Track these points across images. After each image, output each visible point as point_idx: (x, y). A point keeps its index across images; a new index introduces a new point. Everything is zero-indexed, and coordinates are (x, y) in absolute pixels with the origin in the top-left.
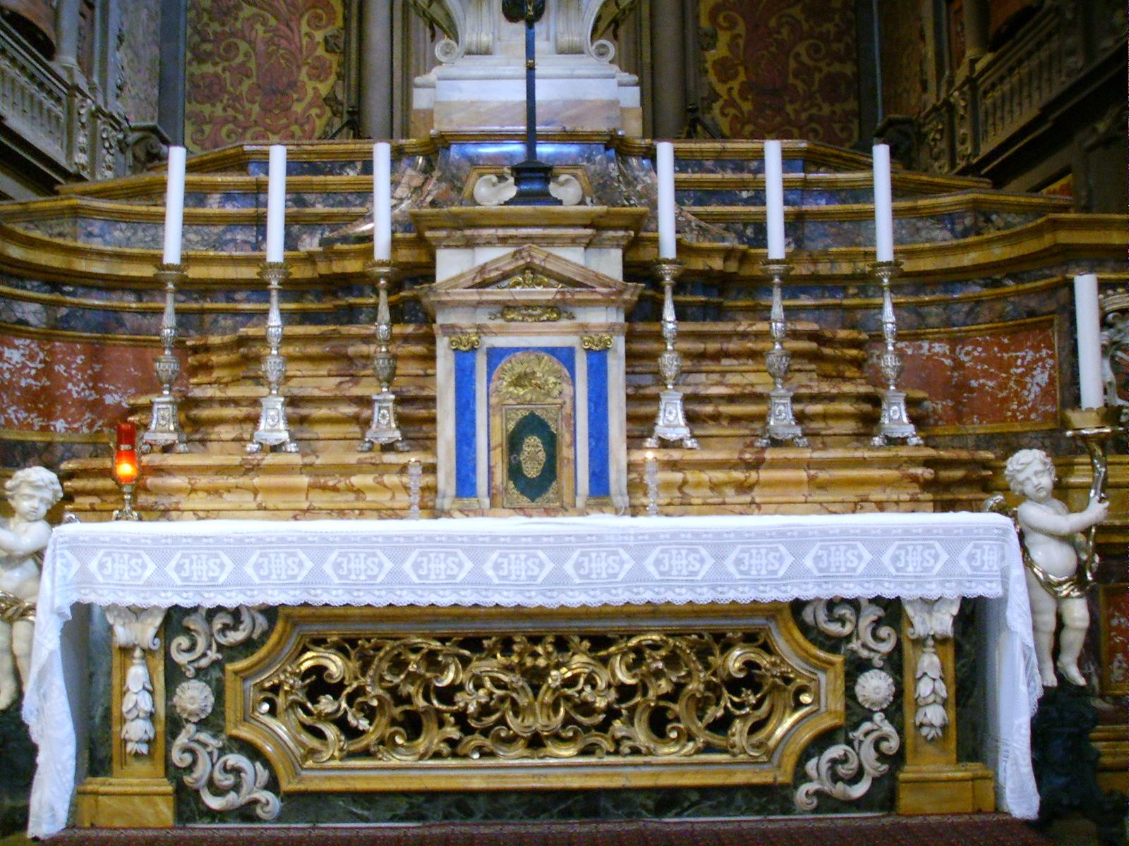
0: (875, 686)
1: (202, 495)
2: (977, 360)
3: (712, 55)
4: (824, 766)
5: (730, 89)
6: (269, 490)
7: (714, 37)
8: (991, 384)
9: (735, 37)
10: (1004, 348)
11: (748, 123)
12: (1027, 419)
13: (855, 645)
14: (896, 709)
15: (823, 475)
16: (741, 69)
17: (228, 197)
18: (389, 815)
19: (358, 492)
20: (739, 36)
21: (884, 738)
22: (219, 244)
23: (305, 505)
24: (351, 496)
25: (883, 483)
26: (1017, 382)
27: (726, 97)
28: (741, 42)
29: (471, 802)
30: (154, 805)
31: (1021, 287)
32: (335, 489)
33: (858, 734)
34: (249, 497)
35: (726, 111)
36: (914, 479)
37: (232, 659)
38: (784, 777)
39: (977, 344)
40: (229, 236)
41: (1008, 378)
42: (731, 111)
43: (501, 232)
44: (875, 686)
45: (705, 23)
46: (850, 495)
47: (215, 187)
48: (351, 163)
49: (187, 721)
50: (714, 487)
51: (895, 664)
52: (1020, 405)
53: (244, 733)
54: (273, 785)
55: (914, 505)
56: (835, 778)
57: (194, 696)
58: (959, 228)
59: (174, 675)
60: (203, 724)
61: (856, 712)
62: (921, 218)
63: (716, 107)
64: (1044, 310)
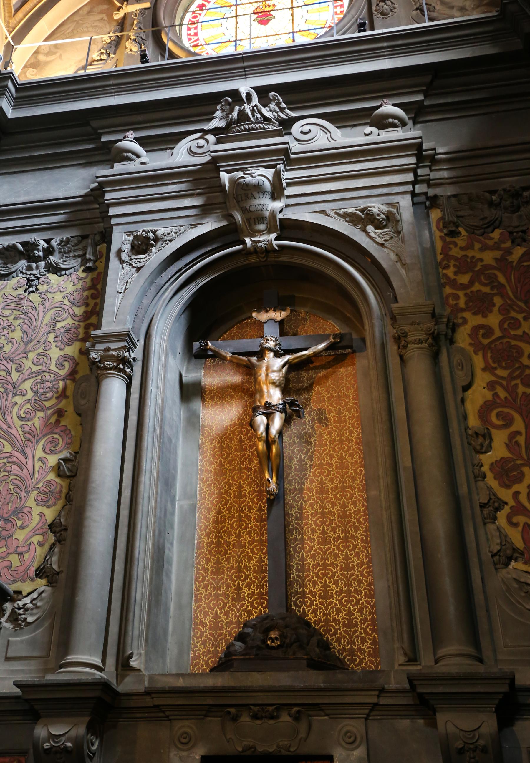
5: (516, 494)
7: (488, 436)
20: (518, 433)
27: (512, 503)
28: (521, 440)
35: (515, 520)
42: (521, 519)
45: (473, 422)
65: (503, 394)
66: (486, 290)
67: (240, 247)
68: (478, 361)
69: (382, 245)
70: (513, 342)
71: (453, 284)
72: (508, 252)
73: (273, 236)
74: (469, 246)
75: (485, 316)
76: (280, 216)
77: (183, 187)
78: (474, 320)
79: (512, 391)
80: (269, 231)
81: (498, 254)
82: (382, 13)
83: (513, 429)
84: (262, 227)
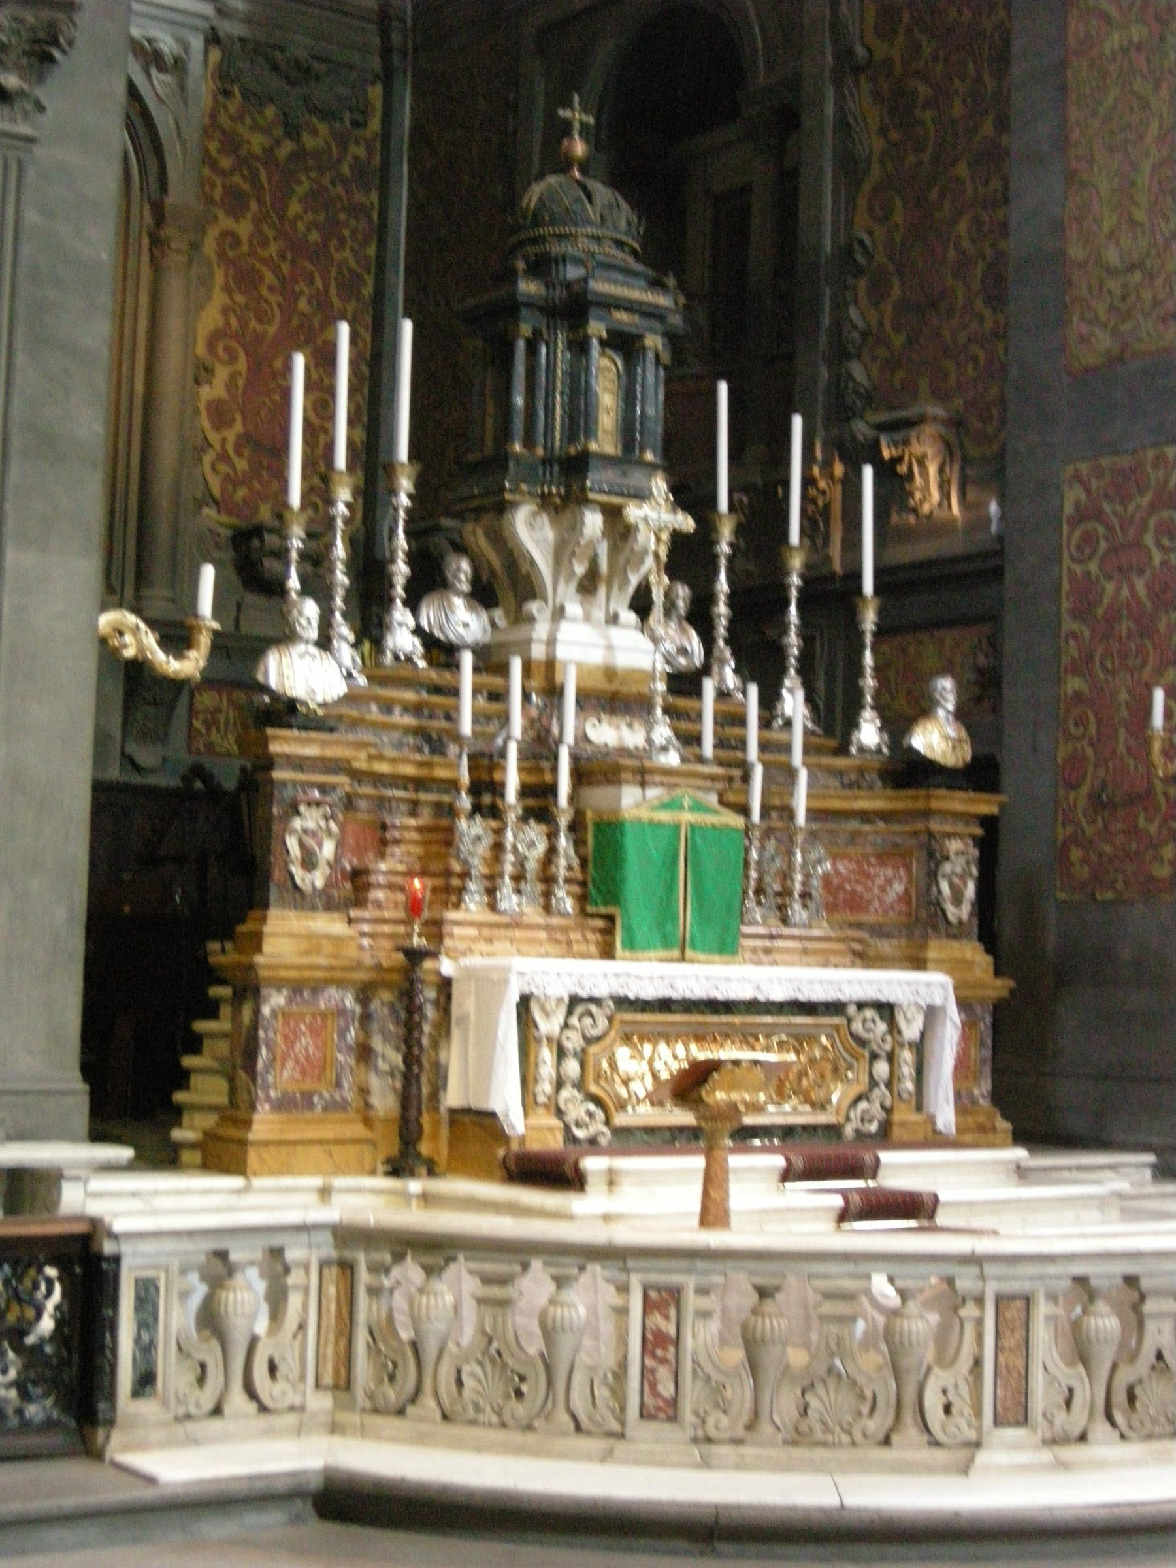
0: (882, 1069)
1: (483, 942)
3: (206, 393)
6: (520, 941)
7: (209, 371)
9: (233, 376)
11: (243, 483)
14: (889, 1085)
15: (810, 945)
16: (238, 417)
27: (218, 447)
28: (241, 382)
34: (507, 945)
38: (841, 1120)
42: (223, 468)
44: (882, 1069)
45: (201, 349)
46: (820, 959)
51: (891, 1058)
53: (594, 1089)
54: (607, 1122)
55: (853, 965)
56: (862, 1120)
58: (846, 780)
59: (561, 1053)
60: (574, 1086)
61: (873, 1083)
63: (208, 458)
65: (234, 323)
66: (246, 187)
68: (219, 277)
70: (258, 265)
71: (214, 165)
72: (278, 143)
74: (239, 118)
75: (237, 220)
78: (226, 222)
79: (244, 324)
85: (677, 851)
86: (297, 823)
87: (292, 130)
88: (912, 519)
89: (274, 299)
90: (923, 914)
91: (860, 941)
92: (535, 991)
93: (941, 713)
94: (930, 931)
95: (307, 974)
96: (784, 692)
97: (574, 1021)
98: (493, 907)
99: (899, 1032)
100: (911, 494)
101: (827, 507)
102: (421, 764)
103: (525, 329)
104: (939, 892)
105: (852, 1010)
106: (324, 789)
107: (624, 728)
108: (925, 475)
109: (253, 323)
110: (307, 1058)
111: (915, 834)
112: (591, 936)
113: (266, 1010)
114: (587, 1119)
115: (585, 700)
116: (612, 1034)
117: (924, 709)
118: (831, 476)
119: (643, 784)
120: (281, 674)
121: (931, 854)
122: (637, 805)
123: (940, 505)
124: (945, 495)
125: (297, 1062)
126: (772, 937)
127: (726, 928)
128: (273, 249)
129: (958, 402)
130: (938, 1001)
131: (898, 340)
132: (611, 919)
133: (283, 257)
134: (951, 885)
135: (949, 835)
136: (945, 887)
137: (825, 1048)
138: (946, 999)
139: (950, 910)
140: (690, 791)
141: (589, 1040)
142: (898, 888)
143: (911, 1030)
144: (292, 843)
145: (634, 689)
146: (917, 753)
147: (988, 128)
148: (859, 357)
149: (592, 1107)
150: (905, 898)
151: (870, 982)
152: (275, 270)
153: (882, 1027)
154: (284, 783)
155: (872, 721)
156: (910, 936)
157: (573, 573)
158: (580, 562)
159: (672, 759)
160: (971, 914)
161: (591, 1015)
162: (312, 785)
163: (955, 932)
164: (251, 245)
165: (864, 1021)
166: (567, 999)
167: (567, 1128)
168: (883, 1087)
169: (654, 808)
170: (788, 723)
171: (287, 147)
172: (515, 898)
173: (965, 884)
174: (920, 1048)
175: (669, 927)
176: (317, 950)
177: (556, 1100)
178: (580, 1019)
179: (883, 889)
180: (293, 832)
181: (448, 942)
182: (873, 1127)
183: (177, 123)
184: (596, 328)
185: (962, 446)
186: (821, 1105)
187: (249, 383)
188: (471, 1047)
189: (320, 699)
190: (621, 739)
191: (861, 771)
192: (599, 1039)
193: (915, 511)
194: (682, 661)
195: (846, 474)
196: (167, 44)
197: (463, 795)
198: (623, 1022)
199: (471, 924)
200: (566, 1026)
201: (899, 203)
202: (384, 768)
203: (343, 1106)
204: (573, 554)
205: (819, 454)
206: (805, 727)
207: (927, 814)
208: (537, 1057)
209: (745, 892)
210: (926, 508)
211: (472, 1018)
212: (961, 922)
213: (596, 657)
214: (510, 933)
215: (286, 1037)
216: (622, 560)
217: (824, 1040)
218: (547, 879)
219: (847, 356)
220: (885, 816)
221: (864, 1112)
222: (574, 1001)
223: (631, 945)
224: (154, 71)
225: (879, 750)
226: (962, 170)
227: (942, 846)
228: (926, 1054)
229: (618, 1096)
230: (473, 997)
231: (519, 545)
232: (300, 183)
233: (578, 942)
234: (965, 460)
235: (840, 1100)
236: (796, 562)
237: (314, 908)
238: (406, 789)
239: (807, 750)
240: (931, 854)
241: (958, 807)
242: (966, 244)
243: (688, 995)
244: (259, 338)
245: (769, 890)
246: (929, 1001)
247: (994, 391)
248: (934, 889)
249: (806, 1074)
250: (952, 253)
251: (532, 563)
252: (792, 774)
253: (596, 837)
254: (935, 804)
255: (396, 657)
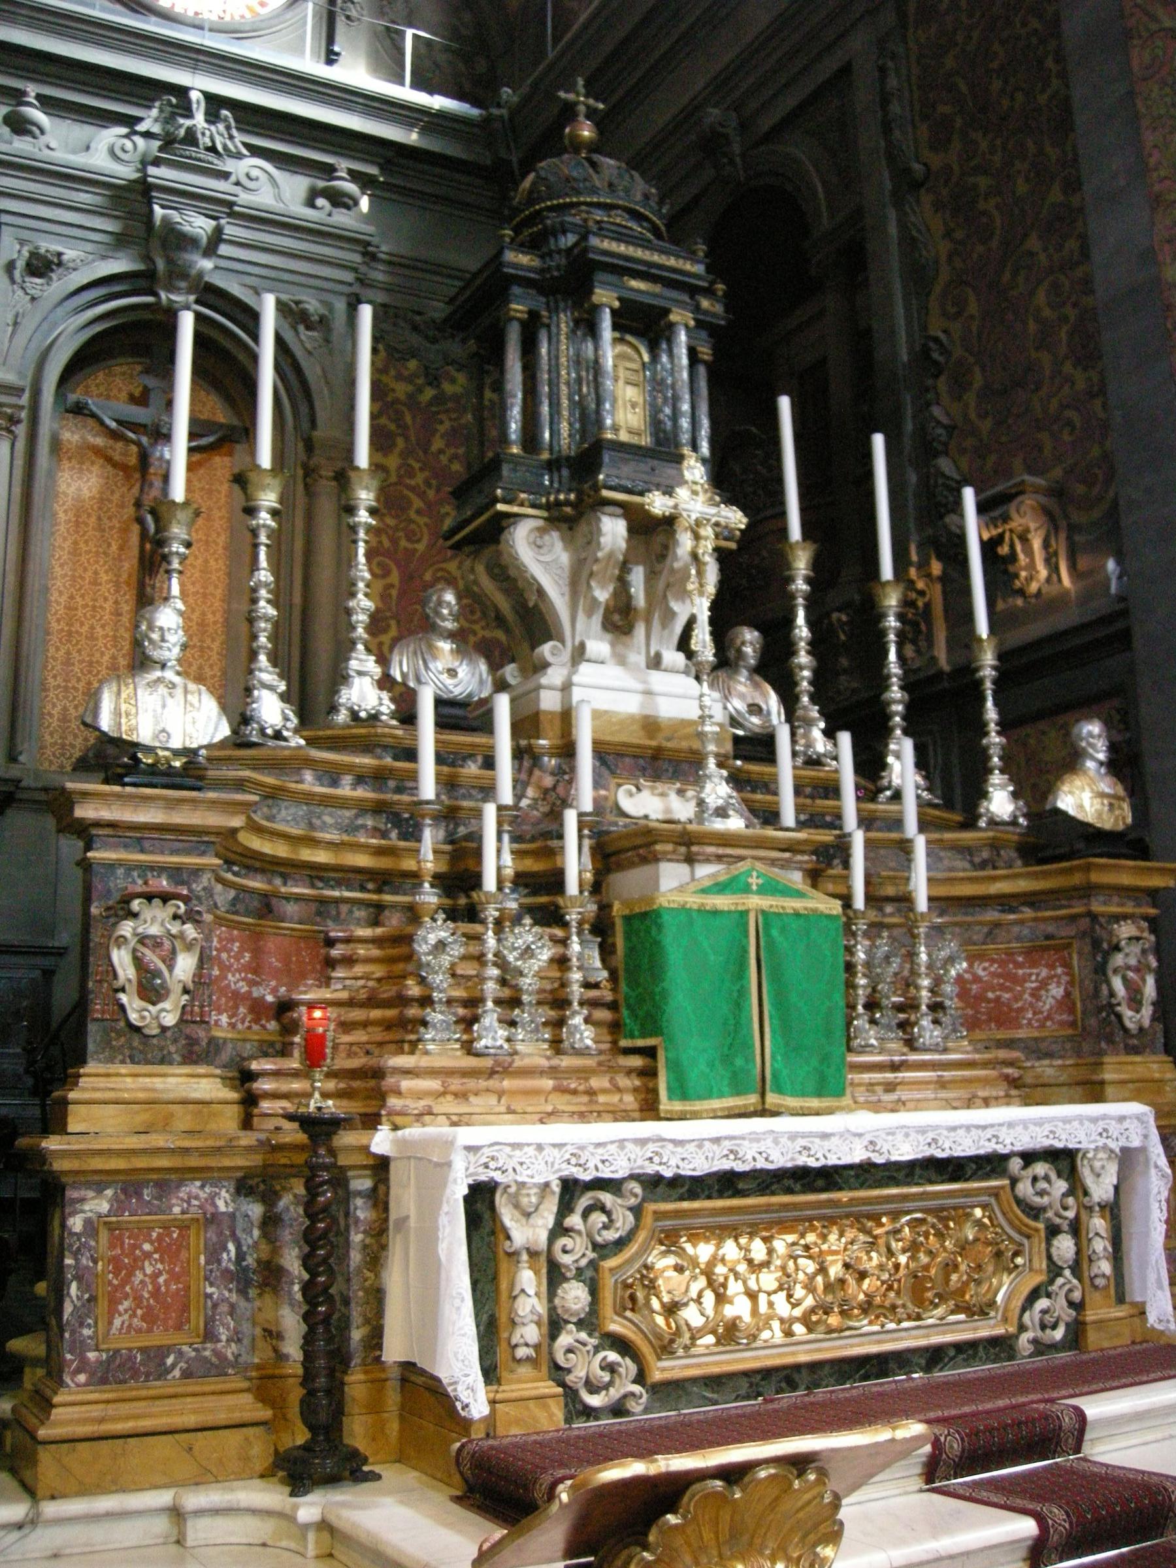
0: (1065, 1246)
1: (449, 1098)
2: (993, 974)
4: (1037, 1317)
6: (513, 1093)
8: (1007, 996)
10: (1019, 965)
12: (1043, 1026)
13: (1050, 1214)
14: (1076, 1268)
16: (393, 623)
17: (360, 780)
18: (734, 1396)
19: (591, 1093)
20: (392, 586)
21: (1070, 1290)
22: (351, 829)
23: (549, 1108)
24: (585, 1099)
25: (985, 1082)
26: (1032, 995)
28: (394, 592)
29: (796, 1377)
30: (546, 1407)
31: (1040, 914)
32: (574, 1092)
33: (1055, 1288)
36: (1006, 1078)
37: (603, 1257)
38: (1012, 1330)
39: (993, 961)
40: (360, 822)
41: (1024, 992)
43: (721, 851)
44: (1065, 1246)
46: (963, 1093)
47: (349, 768)
48: (471, 756)
49: (568, 1322)
50: (871, 1086)
51: (1076, 1229)
52: (1035, 1013)
53: (615, 1326)
54: (640, 1378)
55: (1007, 1100)
56: (1043, 1327)
57: (575, 1295)
58: (977, 860)
59: (555, 1275)
60: (580, 1324)
61: (1055, 1271)
62: (944, 849)
64: (1063, 934)
65: (387, 543)
67: (150, 299)
69: (310, 353)
70: (406, 492)
72: (420, 390)
73: (192, 298)
75: (385, 455)
76: (207, 279)
77: (98, 200)
79: (394, 541)
80: (189, 291)
81: (410, 388)
82: (348, 18)
83: (388, 580)
84: (183, 284)
85: (745, 951)
86: (127, 928)
87: (433, 380)
88: (1020, 602)
89: (422, 520)
90: (1093, 1022)
91: (1011, 1064)
92: (498, 1176)
93: (1090, 764)
94: (1103, 1045)
95: (141, 1163)
96: (890, 759)
97: (574, 1220)
98: (468, 1048)
99: (1086, 1193)
100: (1017, 576)
101: (928, 605)
102: (379, 852)
103: (518, 308)
104: (1112, 994)
105: (1015, 1164)
106: (176, 873)
107: (673, 797)
108: (1029, 553)
109: (403, 543)
110: (156, 1293)
111: (1073, 918)
112: (624, 1082)
113: (76, 1223)
114: (606, 1377)
115: (605, 754)
116: (642, 1236)
117: (1071, 761)
118: (929, 576)
119: (690, 860)
120: (117, 713)
121: (1096, 944)
122: (681, 889)
123: (1048, 580)
124: (1054, 569)
125: (138, 1299)
126: (895, 1067)
127: (825, 1059)
128: (420, 478)
129: (1057, 473)
130: (1136, 1143)
131: (986, 425)
132: (650, 1052)
133: (427, 483)
134: (1125, 980)
135: (1118, 918)
136: (1117, 984)
137: (979, 1223)
138: (1146, 1136)
139: (1127, 1013)
140: (759, 865)
141: (602, 1250)
142: (1056, 991)
143: (1101, 1189)
144: (121, 958)
145: (684, 745)
146: (1064, 814)
147: (1056, 195)
148: (947, 454)
149: (613, 1356)
150: (1066, 1005)
151: (1039, 1123)
152: (422, 495)
153: (1061, 1186)
154: (111, 866)
155: (1003, 787)
156: (1079, 1053)
157: (595, 600)
158: (603, 587)
159: (735, 823)
160: (1154, 1019)
161: (603, 1209)
162: (161, 869)
163: (1136, 1044)
164: (400, 477)
165: (1035, 1179)
166: (556, 1187)
167: (571, 1394)
168: (1067, 1273)
169: (704, 891)
170: (897, 796)
171: (429, 393)
172: (502, 1033)
173: (1144, 981)
174: (1114, 1210)
175: (739, 1062)
176: (165, 1125)
177: (551, 1353)
178: (586, 1214)
179: (1035, 994)
180: (121, 941)
181: (393, 1102)
182: (1058, 1334)
183: (323, 369)
184: (605, 297)
185: (1066, 516)
186: (982, 1310)
187: (402, 593)
188: (411, 1273)
189: (176, 744)
190: (668, 810)
191: (995, 846)
192: (620, 1244)
193: (1021, 592)
194: (755, 720)
195: (944, 572)
196: (313, 305)
197: (427, 885)
198: (659, 1216)
199: (432, 1073)
200: (559, 1230)
201: (972, 298)
202: (321, 857)
203: (219, 1368)
204: (591, 574)
205: (914, 557)
206: (918, 797)
207: (1087, 891)
208: (512, 1285)
209: (852, 1007)
210: (1034, 587)
211: (412, 1223)
212: (1141, 1029)
213: (630, 705)
214: (493, 1083)
215: (115, 1260)
216: (661, 585)
217: (978, 1212)
218: (559, 1002)
219: (936, 454)
220: (1031, 900)
221: (1044, 1312)
222: (570, 1189)
223: (681, 1092)
224: (301, 328)
225: (1014, 822)
226: (1033, 243)
227: (1111, 933)
228: (1124, 1214)
229: (659, 1336)
230: (412, 1189)
231: (522, 569)
232: (441, 422)
233: (604, 1091)
234: (1072, 529)
235: (1009, 1298)
236: (892, 600)
237: (164, 1060)
238: (363, 889)
239: (923, 827)
240: (1096, 944)
241: (1126, 880)
242: (1047, 313)
243: (761, 1164)
244: (410, 553)
245: (885, 1002)
246: (1123, 1142)
247: (1096, 452)
248: (1104, 987)
249: (956, 1267)
250: (1032, 326)
251: (541, 592)
252: (905, 848)
253: (628, 936)
254: (1096, 877)
255: (354, 715)
